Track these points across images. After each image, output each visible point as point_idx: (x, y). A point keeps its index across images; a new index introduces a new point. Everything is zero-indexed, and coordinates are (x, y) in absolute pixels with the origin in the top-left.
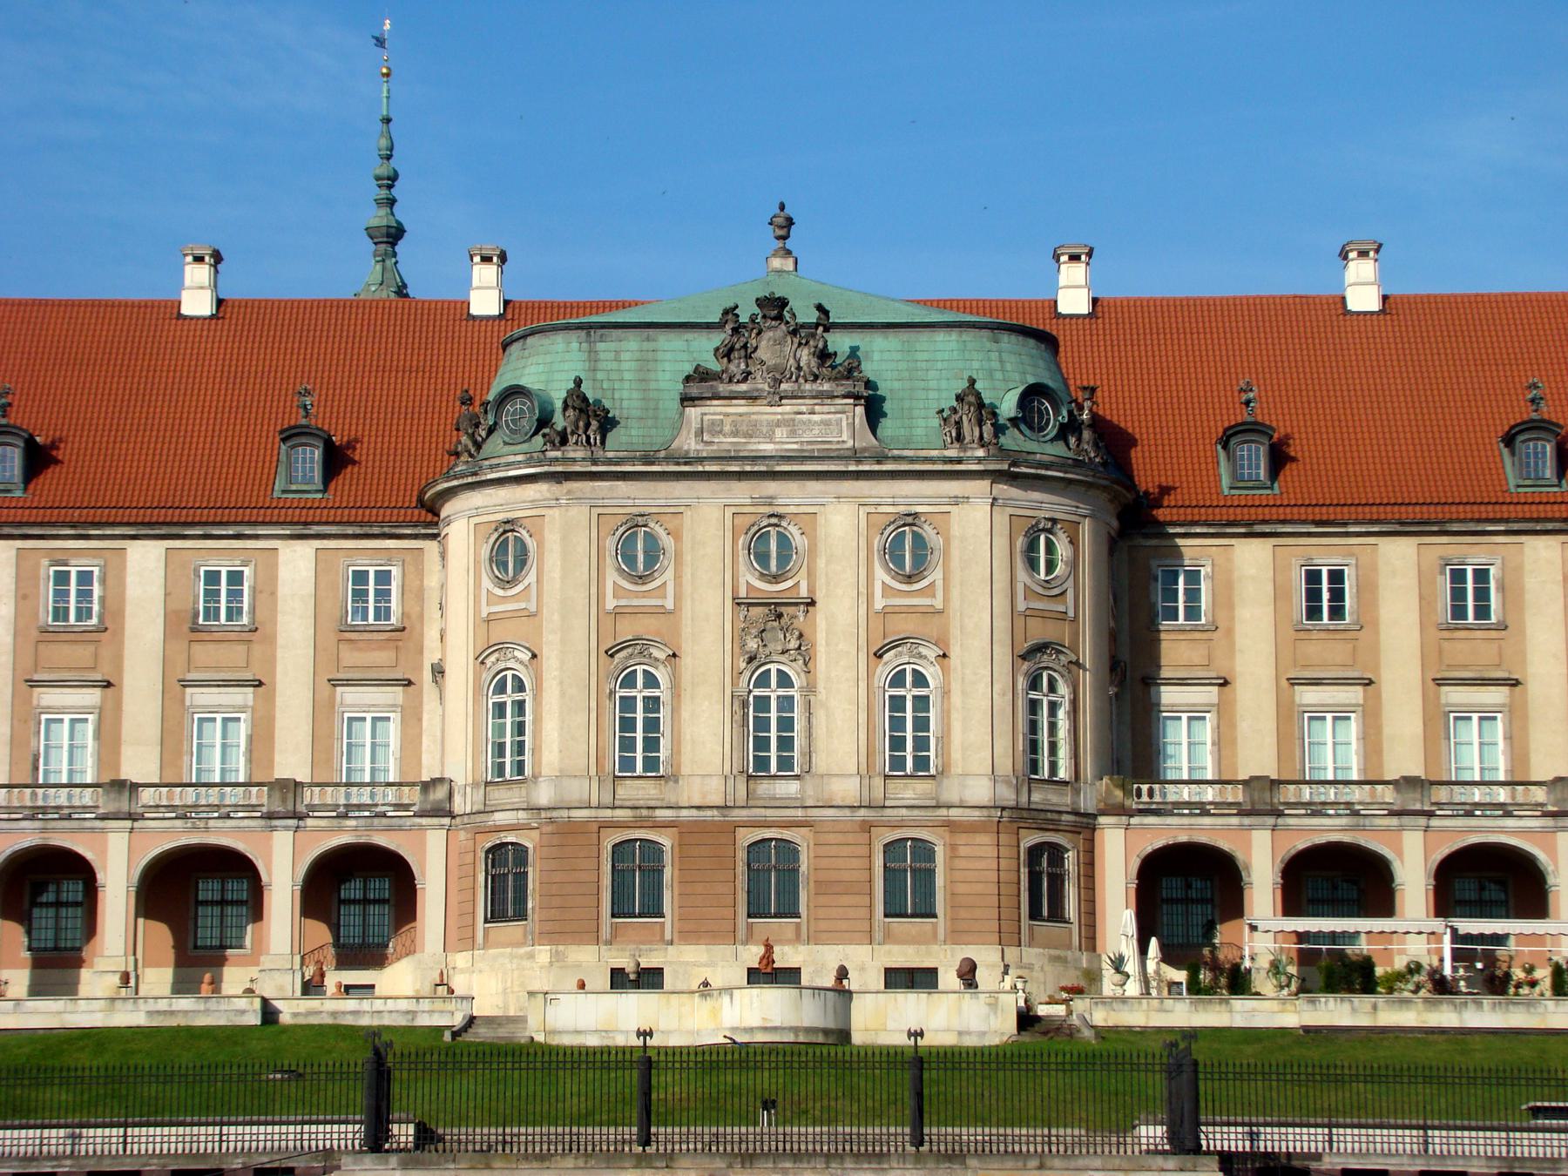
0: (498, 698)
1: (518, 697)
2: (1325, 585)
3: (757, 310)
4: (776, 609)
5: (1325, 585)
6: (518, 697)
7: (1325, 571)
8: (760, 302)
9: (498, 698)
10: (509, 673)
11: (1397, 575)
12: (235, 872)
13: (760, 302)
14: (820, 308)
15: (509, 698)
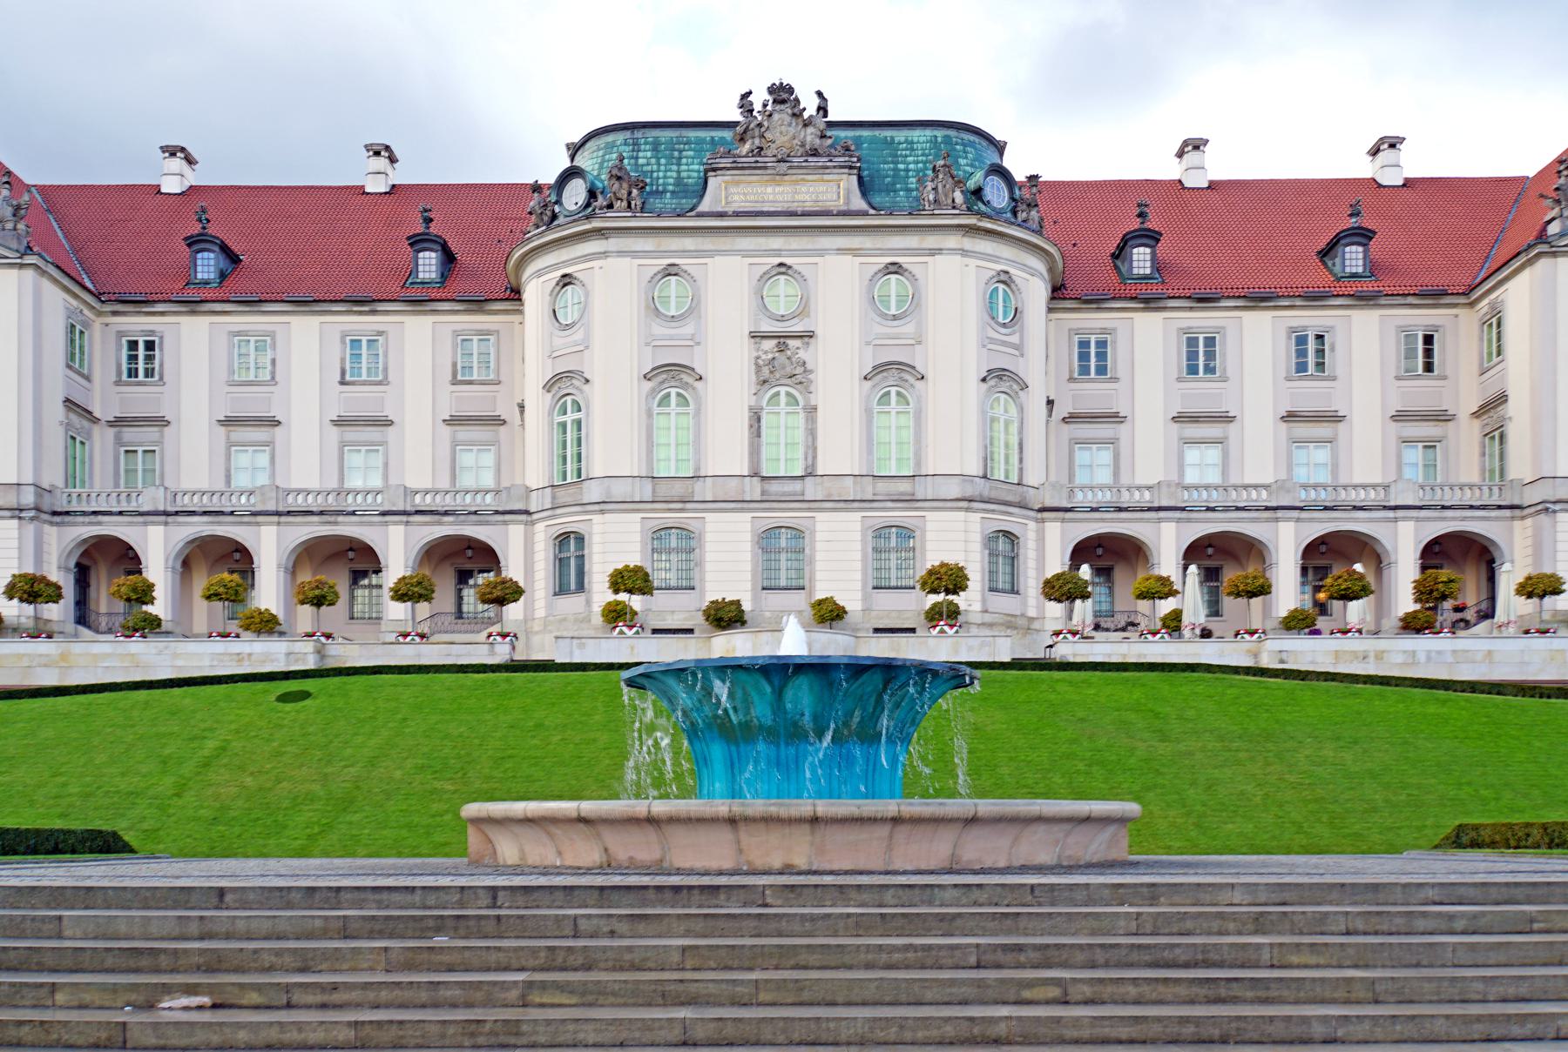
0: (562, 419)
1: (577, 416)
2: (1201, 349)
3: (768, 97)
4: (782, 339)
5: (1201, 349)
6: (577, 416)
7: (1201, 337)
8: (772, 90)
9: (562, 419)
10: (569, 399)
11: (1256, 339)
12: (361, 561)
13: (772, 90)
14: (820, 94)
15: (570, 417)
